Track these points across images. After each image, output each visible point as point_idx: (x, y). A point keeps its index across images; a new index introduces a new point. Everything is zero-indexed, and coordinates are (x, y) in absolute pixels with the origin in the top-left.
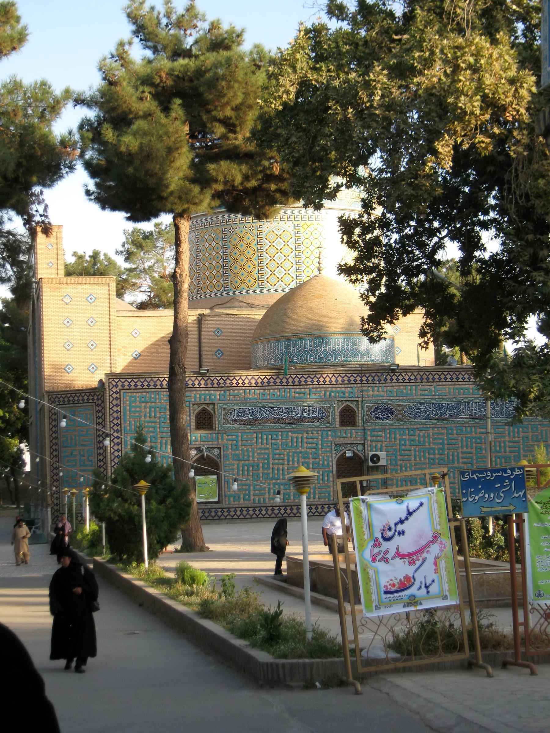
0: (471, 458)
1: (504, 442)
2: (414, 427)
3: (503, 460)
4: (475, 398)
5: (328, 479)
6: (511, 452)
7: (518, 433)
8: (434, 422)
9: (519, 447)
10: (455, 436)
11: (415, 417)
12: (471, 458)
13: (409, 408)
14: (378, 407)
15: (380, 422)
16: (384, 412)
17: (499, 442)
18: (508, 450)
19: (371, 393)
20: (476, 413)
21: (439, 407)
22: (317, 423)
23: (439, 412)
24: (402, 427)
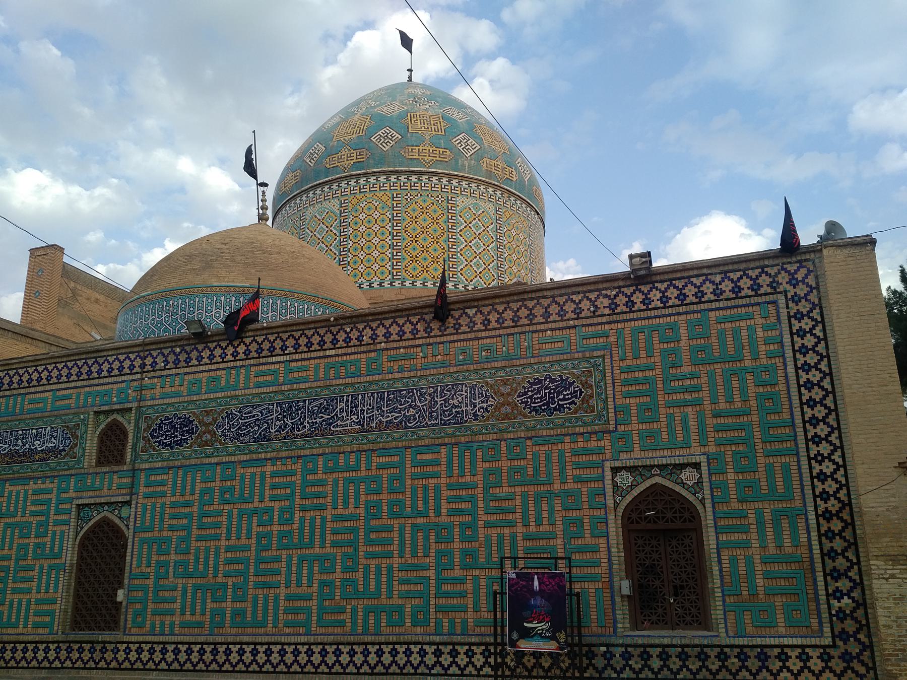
0: (354, 530)
1: (437, 488)
2: (233, 459)
3: (432, 536)
4: (371, 383)
5: (57, 579)
6: (452, 513)
7: (473, 463)
8: (276, 445)
9: (472, 500)
10: (320, 476)
11: (238, 436)
12: (354, 530)
13: (228, 415)
14: (167, 419)
15: (166, 452)
16: (177, 430)
17: (426, 488)
18: (445, 508)
19: (158, 391)
20: (371, 419)
21: (289, 409)
22: (53, 462)
23: (289, 422)
24: (207, 461)
